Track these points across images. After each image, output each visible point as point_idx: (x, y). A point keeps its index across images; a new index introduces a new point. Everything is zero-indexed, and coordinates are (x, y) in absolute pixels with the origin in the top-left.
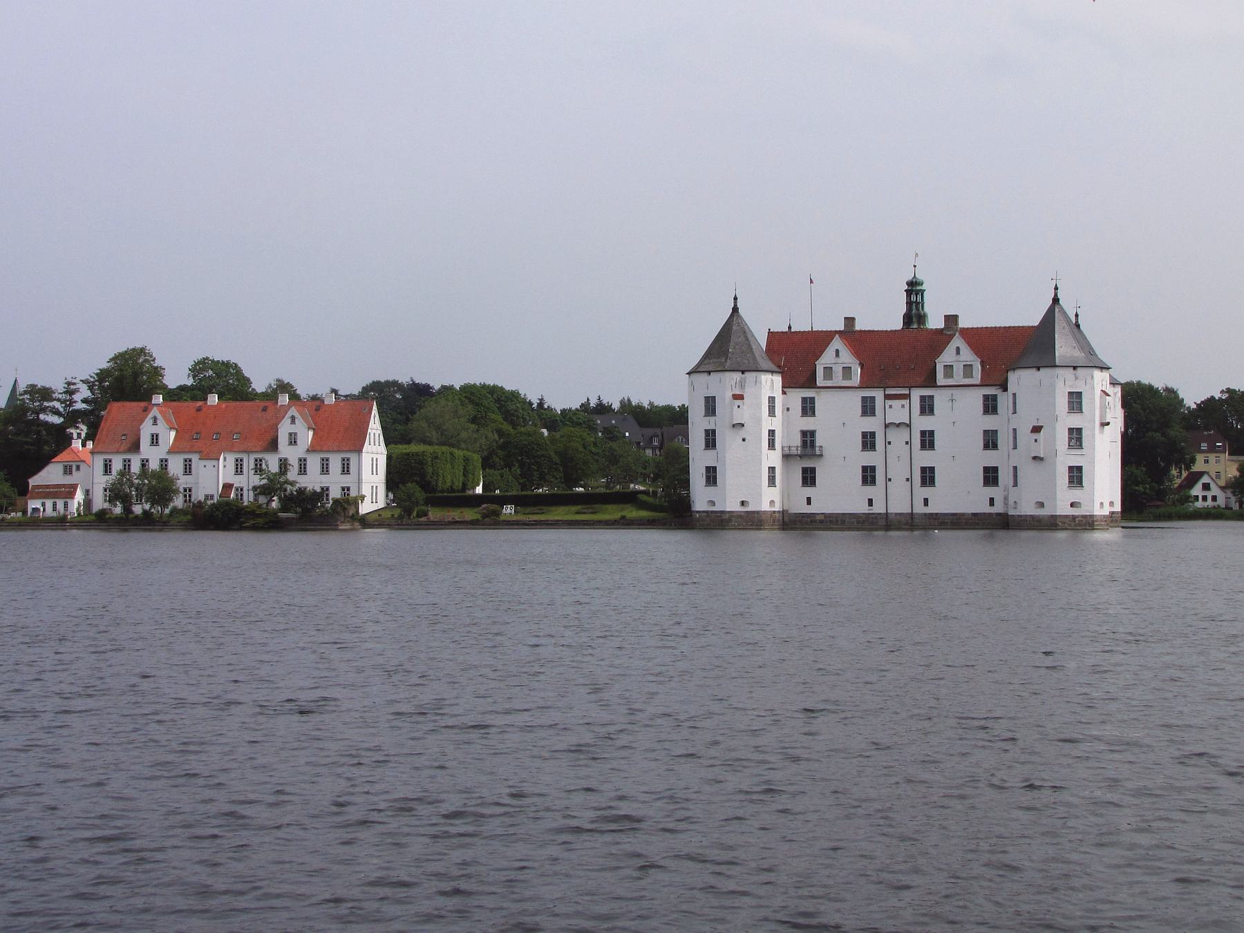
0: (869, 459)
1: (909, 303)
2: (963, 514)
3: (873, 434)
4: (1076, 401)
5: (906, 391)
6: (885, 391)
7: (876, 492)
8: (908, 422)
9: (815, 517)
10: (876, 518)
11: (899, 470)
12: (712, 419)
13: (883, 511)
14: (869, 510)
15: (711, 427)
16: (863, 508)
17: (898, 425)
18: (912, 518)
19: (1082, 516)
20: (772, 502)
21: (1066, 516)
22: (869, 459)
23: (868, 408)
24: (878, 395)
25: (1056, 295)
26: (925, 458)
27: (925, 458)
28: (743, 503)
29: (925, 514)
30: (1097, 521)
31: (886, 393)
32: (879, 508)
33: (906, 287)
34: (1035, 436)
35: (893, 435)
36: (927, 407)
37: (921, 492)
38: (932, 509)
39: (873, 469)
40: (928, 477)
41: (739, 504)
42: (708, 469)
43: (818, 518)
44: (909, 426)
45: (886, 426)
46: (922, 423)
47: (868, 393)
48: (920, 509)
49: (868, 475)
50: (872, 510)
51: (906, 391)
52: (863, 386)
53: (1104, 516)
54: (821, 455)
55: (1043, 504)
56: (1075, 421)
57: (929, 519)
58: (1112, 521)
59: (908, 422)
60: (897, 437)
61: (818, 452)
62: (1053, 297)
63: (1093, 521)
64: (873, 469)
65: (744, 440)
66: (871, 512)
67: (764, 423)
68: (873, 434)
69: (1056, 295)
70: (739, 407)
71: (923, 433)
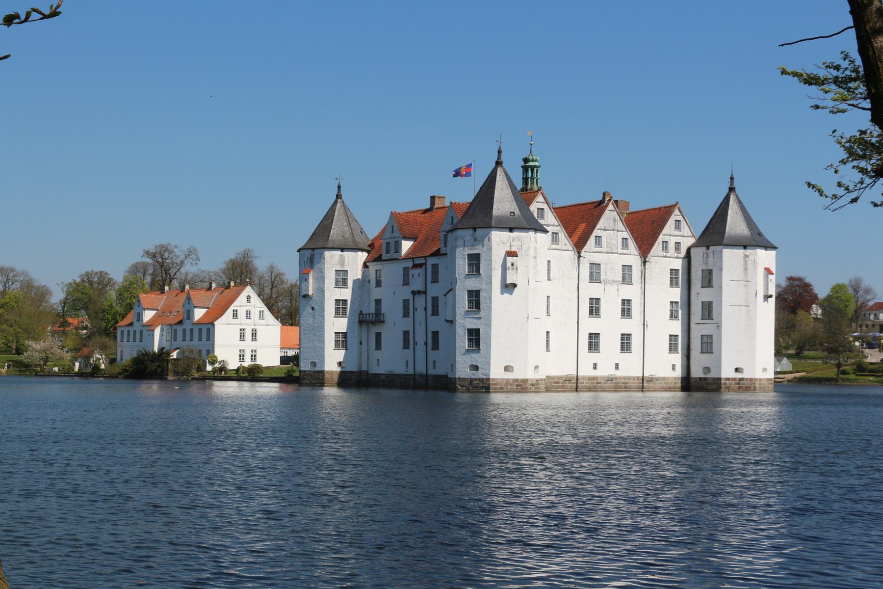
4: (475, 261)
8: (422, 289)
17: (419, 292)
18: (427, 380)
19: (479, 379)
21: (464, 379)
30: (496, 384)
32: (411, 371)
33: (523, 164)
39: (408, 332)
43: (383, 377)
44: (425, 293)
48: (431, 372)
51: (423, 261)
53: (516, 380)
54: (383, 322)
56: (473, 284)
58: (739, 388)
59: (424, 290)
61: (382, 319)
63: (489, 384)
64: (408, 332)
65: (313, 309)
67: (327, 294)
70: (306, 280)
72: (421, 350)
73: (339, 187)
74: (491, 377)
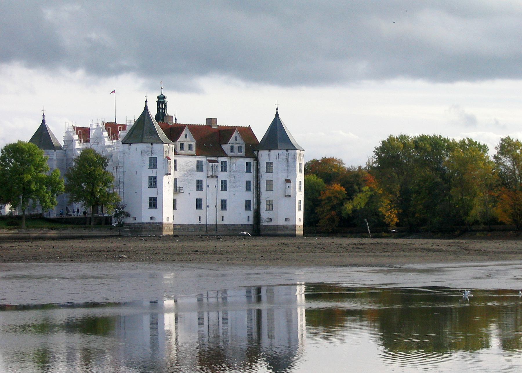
0: (201, 194)
1: (158, 109)
2: (237, 225)
3: (201, 181)
5: (214, 159)
6: (207, 158)
7: (202, 213)
9: (176, 227)
10: (202, 227)
11: (212, 202)
12: (154, 170)
13: (205, 223)
14: (199, 223)
15: (154, 175)
16: (196, 222)
20: (168, 218)
22: (201, 194)
23: (199, 167)
24: (203, 159)
25: (277, 113)
26: (223, 195)
27: (223, 195)
28: (151, 218)
29: (222, 225)
31: (208, 159)
32: (203, 222)
34: (288, 184)
35: (210, 180)
36: (224, 168)
37: (221, 213)
38: (225, 222)
40: (224, 205)
41: (149, 219)
42: (150, 199)
44: (217, 177)
45: (208, 177)
46: (222, 176)
47: (199, 159)
48: (220, 222)
49: (199, 204)
50: (200, 223)
52: (198, 154)
55: (271, 219)
57: (224, 227)
60: (212, 182)
62: (276, 113)
66: (200, 224)
68: (201, 181)
69: (277, 113)
71: (222, 181)
72: (212, 210)
73: (146, 101)
74: (296, 224)
